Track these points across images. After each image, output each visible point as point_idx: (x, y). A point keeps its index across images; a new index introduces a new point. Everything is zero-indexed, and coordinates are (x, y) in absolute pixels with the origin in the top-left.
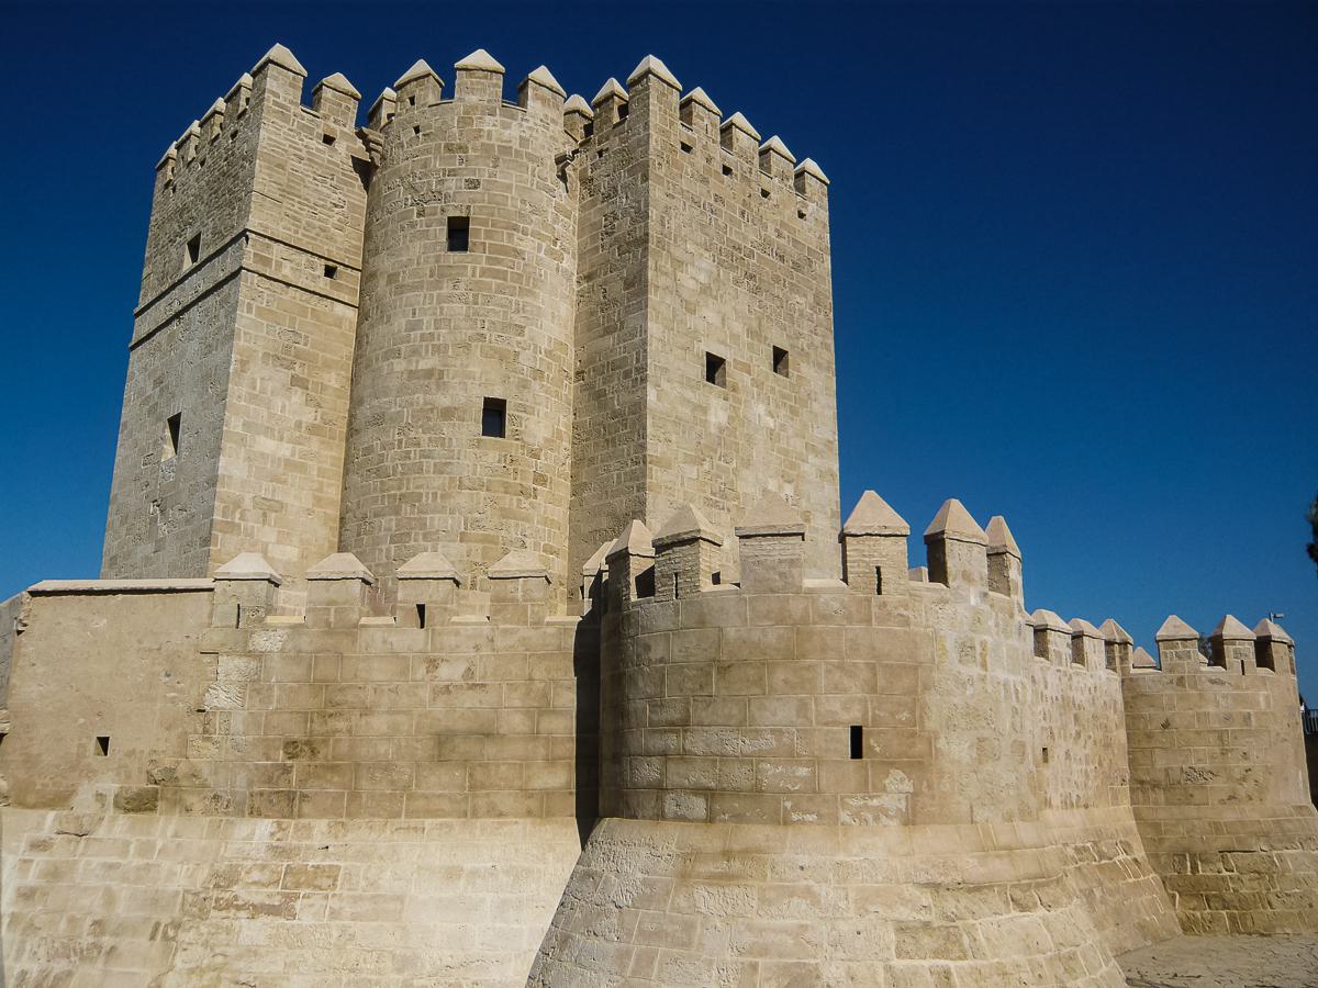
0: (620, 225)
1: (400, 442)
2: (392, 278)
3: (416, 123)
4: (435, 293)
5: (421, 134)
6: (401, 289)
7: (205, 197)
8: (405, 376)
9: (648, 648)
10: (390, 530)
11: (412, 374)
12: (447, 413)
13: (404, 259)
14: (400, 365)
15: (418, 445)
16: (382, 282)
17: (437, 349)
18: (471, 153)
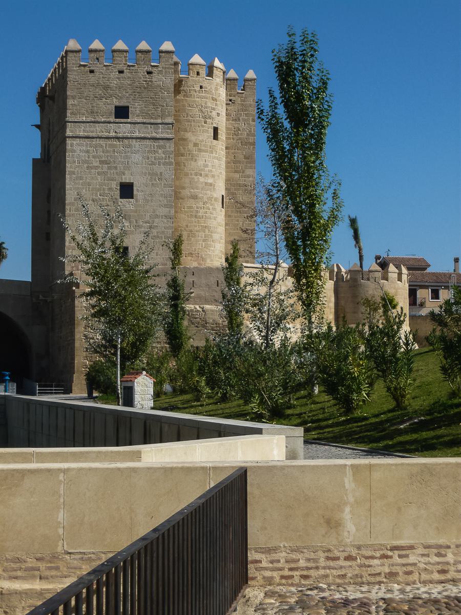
0: (241, 134)
1: (204, 207)
2: (196, 145)
3: (202, 84)
4: (212, 155)
5: (203, 89)
6: (200, 150)
7: (130, 92)
8: (204, 184)
9: (367, 291)
10: (202, 237)
11: (206, 183)
12: (216, 199)
13: (201, 139)
14: (202, 179)
15: (209, 209)
16: (191, 146)
17: (213, 176)
18: (218, 102)
